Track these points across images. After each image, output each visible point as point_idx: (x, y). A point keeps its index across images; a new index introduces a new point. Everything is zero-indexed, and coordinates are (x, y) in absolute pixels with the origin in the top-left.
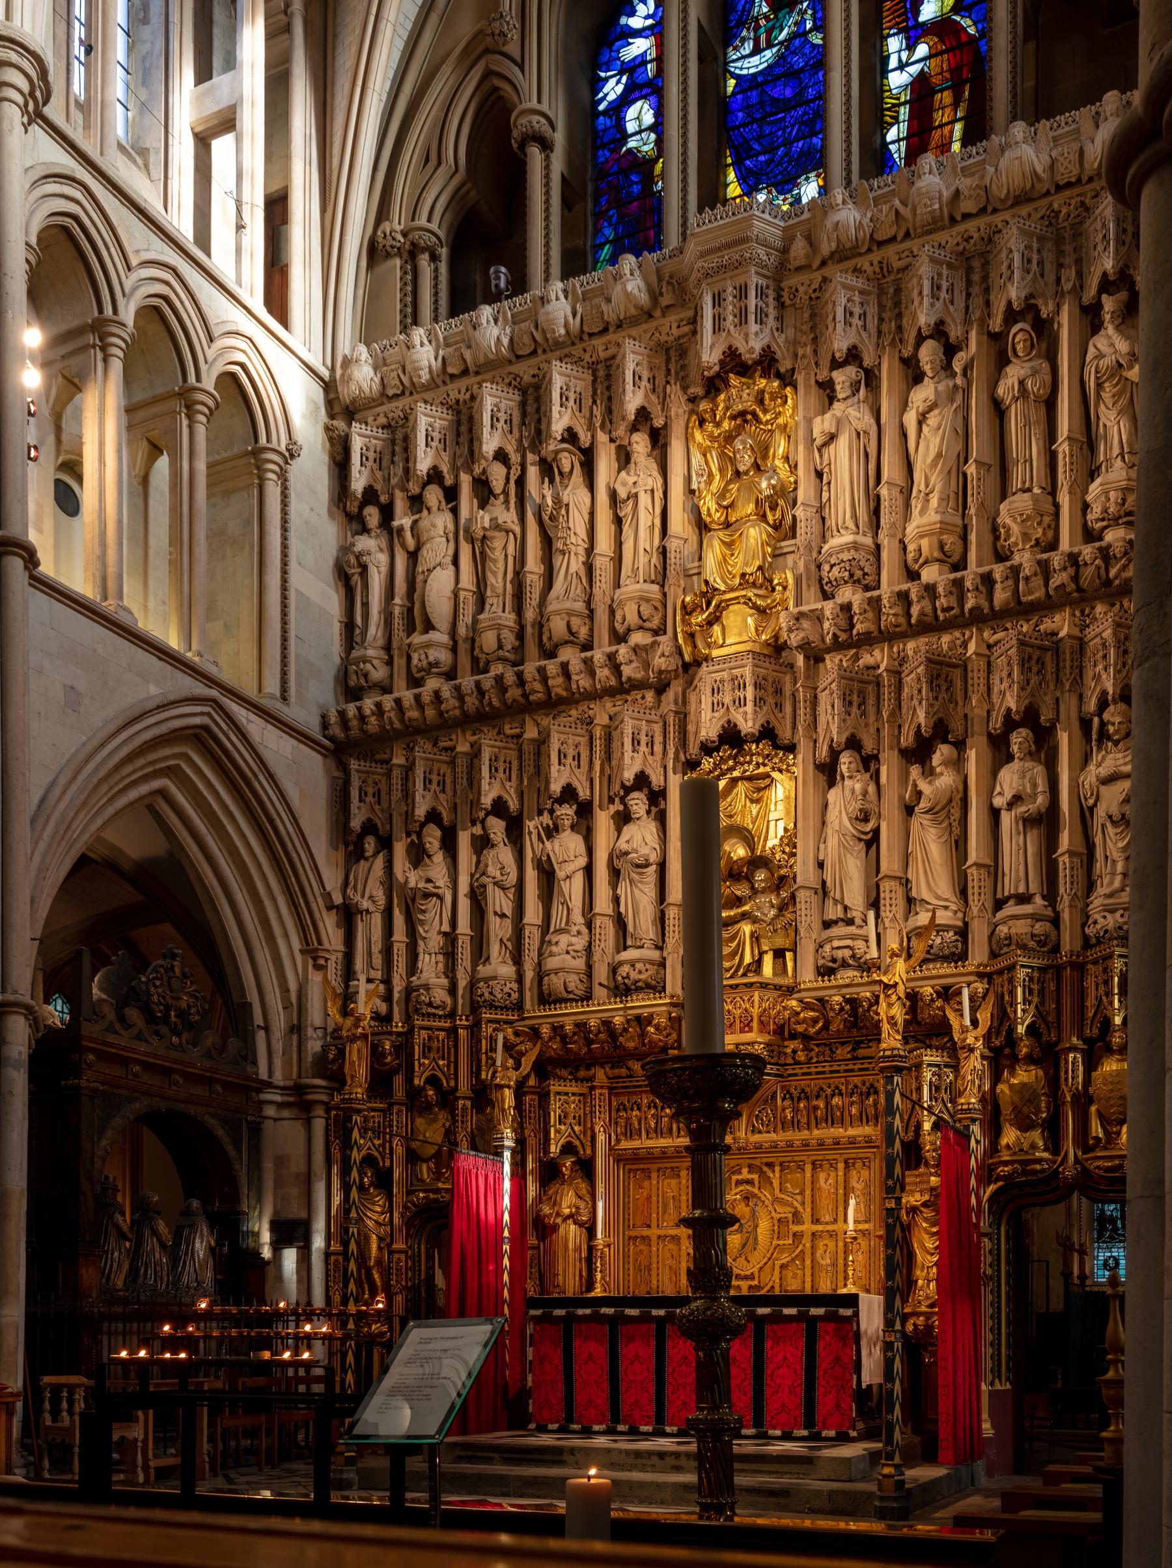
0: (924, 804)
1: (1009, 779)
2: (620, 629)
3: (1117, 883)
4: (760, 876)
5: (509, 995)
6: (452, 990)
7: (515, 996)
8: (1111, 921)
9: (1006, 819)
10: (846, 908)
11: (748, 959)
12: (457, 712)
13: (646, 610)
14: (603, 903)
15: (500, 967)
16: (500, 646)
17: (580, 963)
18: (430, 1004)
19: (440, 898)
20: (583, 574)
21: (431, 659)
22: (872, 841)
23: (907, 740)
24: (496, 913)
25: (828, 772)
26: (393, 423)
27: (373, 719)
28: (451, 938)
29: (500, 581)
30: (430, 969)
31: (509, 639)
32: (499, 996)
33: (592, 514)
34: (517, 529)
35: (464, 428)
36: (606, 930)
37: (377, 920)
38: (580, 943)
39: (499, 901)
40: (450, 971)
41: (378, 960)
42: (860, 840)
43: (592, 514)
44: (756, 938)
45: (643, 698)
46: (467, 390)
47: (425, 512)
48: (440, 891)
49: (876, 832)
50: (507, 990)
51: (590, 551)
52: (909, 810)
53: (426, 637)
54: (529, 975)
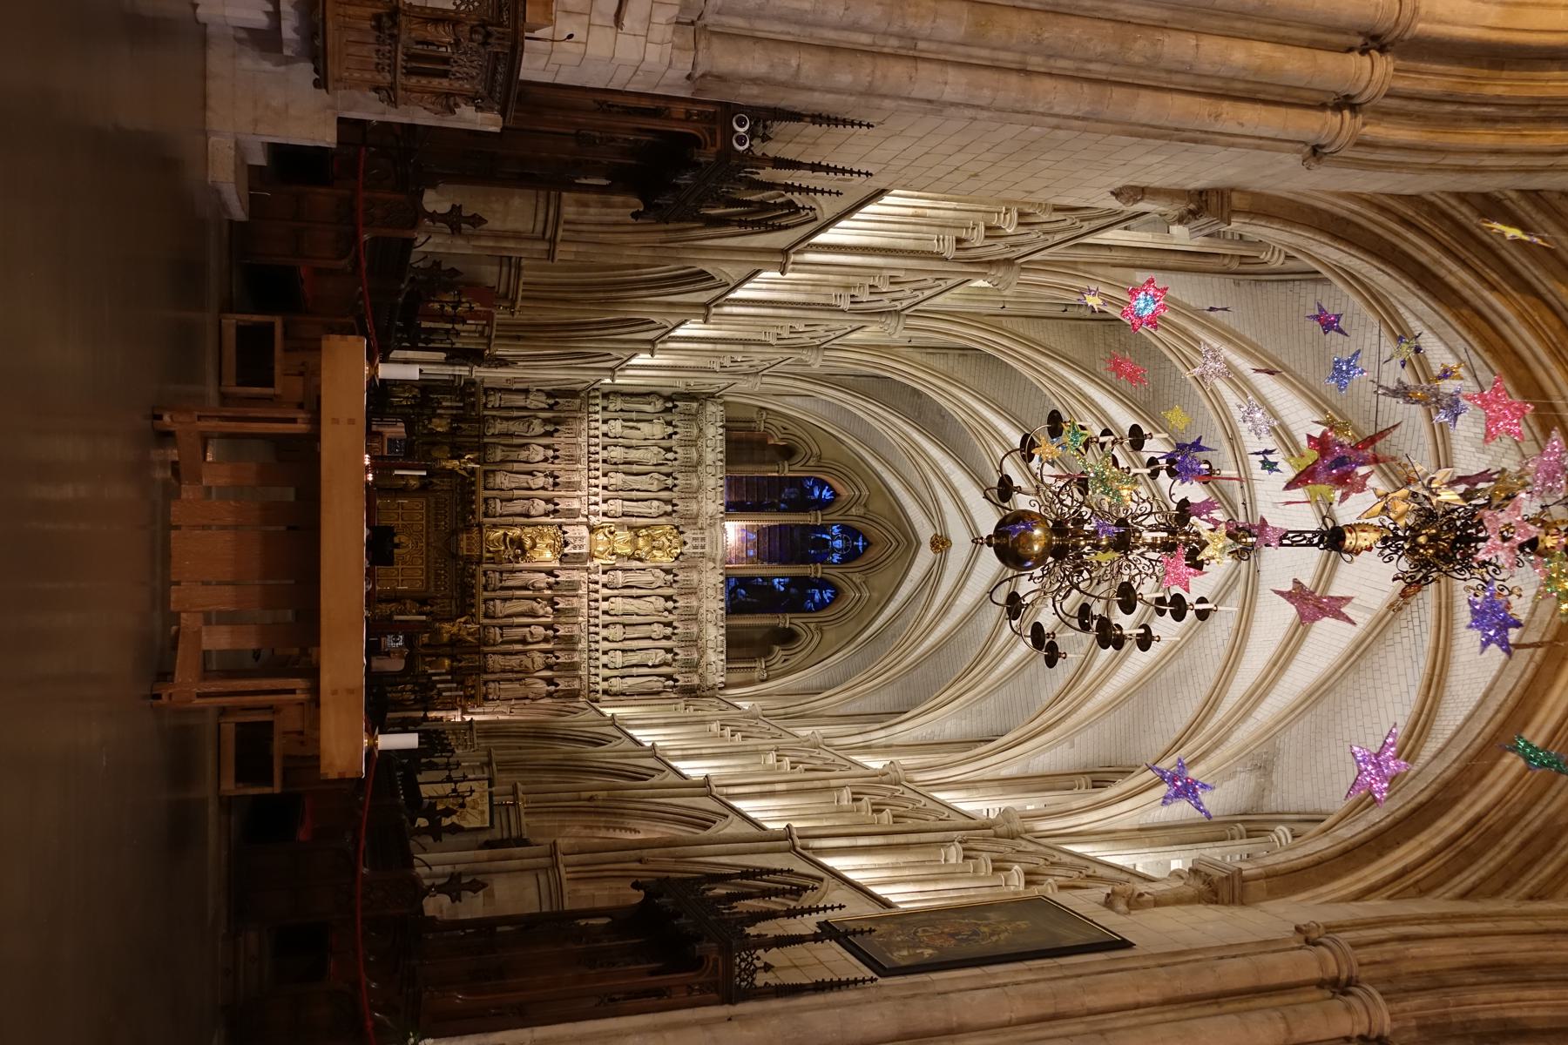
2: (610, 502)
8: (490, 662)
9: (528, 629)
15: (499, 455)
22: (525, 588)
23: (556, 599)
25: (550, 573)
28: (512, 435)
29: (633, 455)
35: (690, 443)
36: (509, 494)
37: (522, 404)
39: (523, 455)
40: (500, 435)
41: (509, 404)
49: (529, 589)
51: (638, 490)
52: (534, 599)
54: (494, 468)
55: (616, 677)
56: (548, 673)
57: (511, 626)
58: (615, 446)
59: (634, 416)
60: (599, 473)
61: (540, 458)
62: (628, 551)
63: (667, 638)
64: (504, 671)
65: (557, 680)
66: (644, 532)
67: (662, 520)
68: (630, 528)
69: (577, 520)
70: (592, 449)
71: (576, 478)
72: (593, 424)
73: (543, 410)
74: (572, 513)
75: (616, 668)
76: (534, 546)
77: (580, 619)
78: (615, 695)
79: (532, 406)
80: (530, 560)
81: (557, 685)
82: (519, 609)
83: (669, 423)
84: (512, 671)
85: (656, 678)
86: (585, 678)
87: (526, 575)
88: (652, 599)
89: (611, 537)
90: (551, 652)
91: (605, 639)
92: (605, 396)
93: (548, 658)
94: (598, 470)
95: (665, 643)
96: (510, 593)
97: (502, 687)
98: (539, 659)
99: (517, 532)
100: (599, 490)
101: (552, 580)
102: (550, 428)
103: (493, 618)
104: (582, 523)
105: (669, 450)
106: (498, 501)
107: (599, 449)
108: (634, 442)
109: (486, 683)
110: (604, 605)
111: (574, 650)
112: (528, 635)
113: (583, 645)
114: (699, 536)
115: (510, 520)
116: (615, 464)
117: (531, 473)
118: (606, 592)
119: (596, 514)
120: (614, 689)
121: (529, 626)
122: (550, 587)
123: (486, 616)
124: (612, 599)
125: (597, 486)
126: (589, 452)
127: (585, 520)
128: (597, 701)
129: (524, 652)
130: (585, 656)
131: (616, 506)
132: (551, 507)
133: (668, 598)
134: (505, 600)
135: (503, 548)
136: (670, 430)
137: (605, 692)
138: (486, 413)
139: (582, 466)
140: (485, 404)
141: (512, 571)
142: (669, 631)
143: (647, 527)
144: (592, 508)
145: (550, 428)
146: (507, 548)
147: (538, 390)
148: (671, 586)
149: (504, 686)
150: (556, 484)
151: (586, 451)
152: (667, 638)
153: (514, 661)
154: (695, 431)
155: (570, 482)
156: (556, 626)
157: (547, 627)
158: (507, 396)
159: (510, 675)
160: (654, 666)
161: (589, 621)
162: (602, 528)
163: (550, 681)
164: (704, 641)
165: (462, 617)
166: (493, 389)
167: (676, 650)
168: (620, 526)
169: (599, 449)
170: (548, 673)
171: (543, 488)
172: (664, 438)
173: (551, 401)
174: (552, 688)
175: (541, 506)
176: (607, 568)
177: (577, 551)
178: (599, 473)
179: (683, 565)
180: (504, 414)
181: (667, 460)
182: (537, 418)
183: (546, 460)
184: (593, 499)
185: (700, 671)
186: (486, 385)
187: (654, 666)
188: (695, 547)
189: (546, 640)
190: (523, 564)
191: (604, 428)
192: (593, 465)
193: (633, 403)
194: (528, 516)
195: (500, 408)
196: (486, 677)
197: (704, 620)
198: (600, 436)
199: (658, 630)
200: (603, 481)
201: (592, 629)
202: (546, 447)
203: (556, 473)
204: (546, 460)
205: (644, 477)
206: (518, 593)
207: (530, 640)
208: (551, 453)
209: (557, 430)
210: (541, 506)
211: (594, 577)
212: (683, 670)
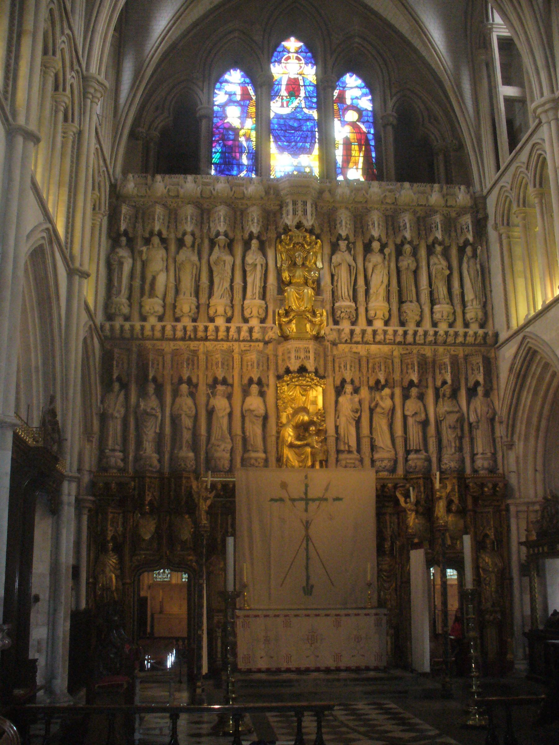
0: (378, 410)
1: (412, 406)
3: (453, 450)
4: (312, 428)
5: (192, 466)
6: (159, 461)
7: (194, 467)
9: (410, 421)
10: (349, 446)
11: (309, 463)
12: (172, 337)
13: (261, 311)
14: (237, 430)
16: (190, 312)
17: (228, 455)
18: (151, 466)
19: (156, 417)
20: (229, 288)
21: (156, 310)
22: (358, 422)
23: (372, 383)
24: (186, 428)
25: (339, 391)
26: (137, 206)
27: (128, 332)
28: (160, 436)
29: (187, 284)
30: (149, 447)
31: (194, 310)
32: (189, 466)
33: (233, 265)
34: (198, 264)
37: (119, 422)
38: (229, 447)
39: (187, 422)
42: (354, 420)
43: (233, 265)
44: (313, 455)
45: (258, 346)
46: (176, 202)
47: (151, 247)
48: (158, 414)
49: (360, 418)
50: (191, 463)
51: (232, 281)
53: (152, 300)
55: (464, 314)
56: (463, 393)
57: (406, 440)
58: (175, 307)
59: (137, 283)
60: (211, 326)
61: (189, 401)
62: (308, 291)
63: (415, 253)
64: (460, 449)
65: (471, 384)
66: (286, 275)
67: (270, 253)
68: (281, 291)
69: (271, 357)
70: (179, 334)
72: (148, 332)
73: (127, 398)
75: (454, 313)
76: (304, 410)
77: (396, 353)
78: (485, 314)
79: (123, 411)
80: (323, 414)
81: (477, 383)
82: (385, 428)
83: (147, 241)
84: (461, 438)
85: (465, 266)
86: (468, 350)
87: (343, 421)
88: (370, 266)
89: (292, 314)
90: (437, 391)
91: (418, 324)
92: (110, 317)
93: (444, 395)
94: (206, 328)
95: (423, 252)
97: (480, 450)
98: (445, 407)
99: (289, 434)
100: (233, 326)
101: (349, 388)
102: (151, 388)
103: (396, 461)
104: (276, 350)
105: (181, 243)
106: (246, 455)
107: (179, 326)
108: (172, 284)
109: (475, 471)
110: (379, 324)
111: (434, 361)
112: (418, 419)
113: (428, 351)
114: (290, 207)
116: (198, 307)
117: (210, 413)
118: (362, 320)
120: (480, 315)
121: (405, 418)
122: (356, 391)
123: (393, 470)
124: (371, 313)
125: (228, 329)
126: (183, 339)
127: (271, 346)
128: (496, 335)
130: (441, 349)
132: (254, 388)
134: (373, 448)
135: (309, 450)
136: (156, 240)
138: (131, 470)
139: (202, 347)
140: (120, 470)
141: (337, 439)
143: (279, 272)
144: (256, 335)
145: (151, 388)
146: (307, 445)
147: (102, 402)
148: (354, 243)
149: (479, 448)
150: (224, 382)
151: (181, 343)
152: (415, 253)
153: (448, 435)
155: (223, 364)
156: (406, 384)
158: (110, 442)
159: (466, 441)
160: (450, 268)
161: (399, 343)
162: (280, 325)
163: (472, 392)
164: (418, 209)
165: (397, 501)
166: (100, 460)
167: (431, 240)
169: (179, 326)
170: (463, 393)
171: (229, 397)
172: (167, 249)
173: (116, 386)
174: (480, 390)
176: (331, 320)
177: (312, 356)
178: (211, 326)
179: (326, 229)
180: (132, 447)
181: (193, 246)
182: (138, 405)
183: (192, 395)
184: (244, 334)
185: (453, 215)
186: (94, 469)
187: (450, 268)
188: (305, 212)
189: (421, 397)
190: (330, 426)
191: (152, 320)
192: (200, 334)
193: (120, 282)
194: (265, 418)
195: (124, 451)
196: (468, 470)
197: (392, 207)
198: (163, 324)
199: (407, 262)
200: (220, 322)
201: (410, 339)
202: (176, 393)
203: (210, 381)
204: (192, 395)
205: (215, 274)
206: (365, 431)
207: (423, 416)
208: (184, 388)
209: (155, 380)
211: (345, 335)
212: (453, 234)
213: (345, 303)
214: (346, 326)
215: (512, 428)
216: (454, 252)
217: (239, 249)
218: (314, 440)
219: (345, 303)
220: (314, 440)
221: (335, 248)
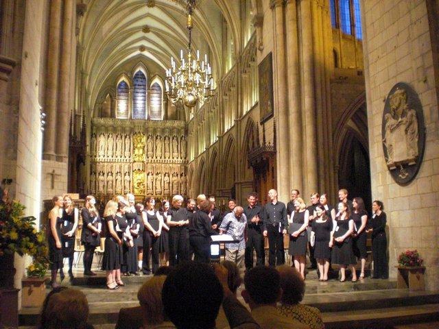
1: (167, 178)
25: (148, 175)
28: (104, 186)
63: (169, 139)
68: (134, 149)
71: (118, 166)
74: (129, 168)
95: (171, 139)
96: (154, 188)
98: (175, 178)
99: (136, 185)
101: (150, 174)
110: (159, 158)
115: (131, 187)
118: (154, 157)
119: (130, 160)
123: (161, 194)
129: (173, 183)
131: (127, 153)
133: (157, 138)
137: (185, 158)
142: (167, 138)
154: (103, 128)
157: (165, 175)
163: (181, 175)
168: (134, 152)
175: (127, 177)
189: (169, 176)
190: (145, 183)
199: (167, 142)
200: (119, 157)
210: (127, 177)
211: (150, 161)
213: (150, 153)
214: (150, 158)
215: (190, 185)
216: (179, 139)
217: (123, 138)
218: (142, 187)
219: (150, 153)
220: (142, 187)
221: (148, 138)
